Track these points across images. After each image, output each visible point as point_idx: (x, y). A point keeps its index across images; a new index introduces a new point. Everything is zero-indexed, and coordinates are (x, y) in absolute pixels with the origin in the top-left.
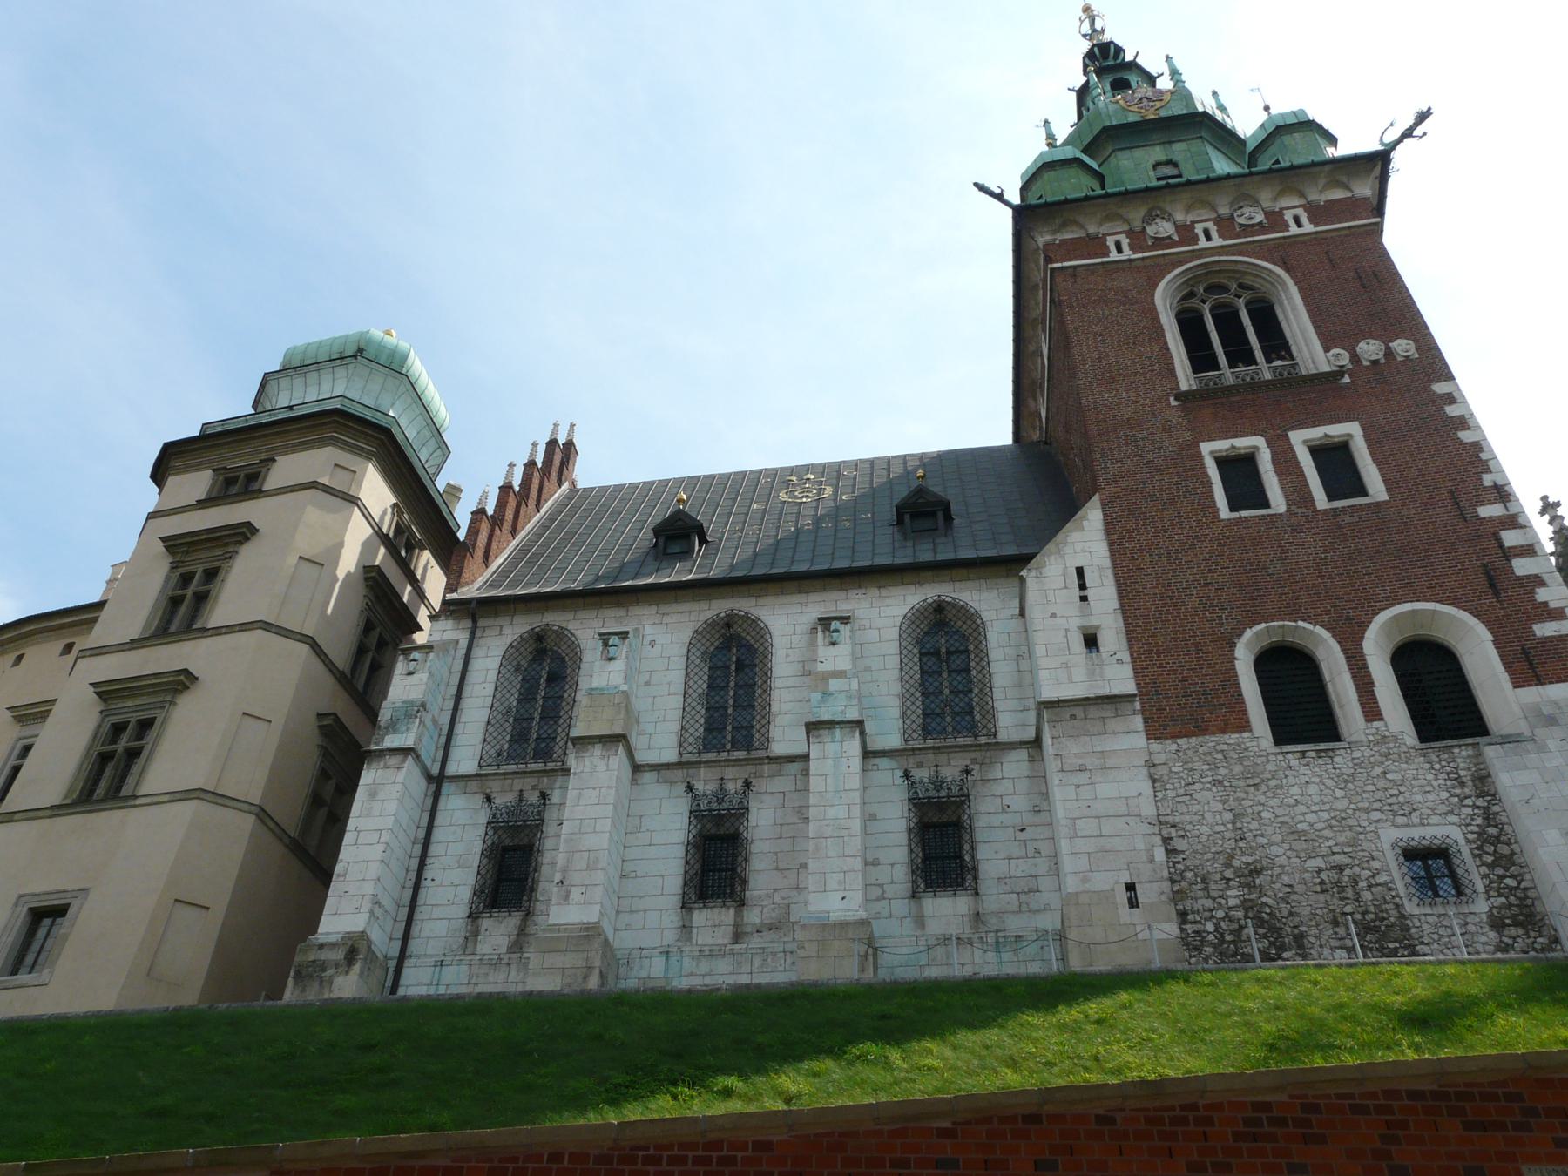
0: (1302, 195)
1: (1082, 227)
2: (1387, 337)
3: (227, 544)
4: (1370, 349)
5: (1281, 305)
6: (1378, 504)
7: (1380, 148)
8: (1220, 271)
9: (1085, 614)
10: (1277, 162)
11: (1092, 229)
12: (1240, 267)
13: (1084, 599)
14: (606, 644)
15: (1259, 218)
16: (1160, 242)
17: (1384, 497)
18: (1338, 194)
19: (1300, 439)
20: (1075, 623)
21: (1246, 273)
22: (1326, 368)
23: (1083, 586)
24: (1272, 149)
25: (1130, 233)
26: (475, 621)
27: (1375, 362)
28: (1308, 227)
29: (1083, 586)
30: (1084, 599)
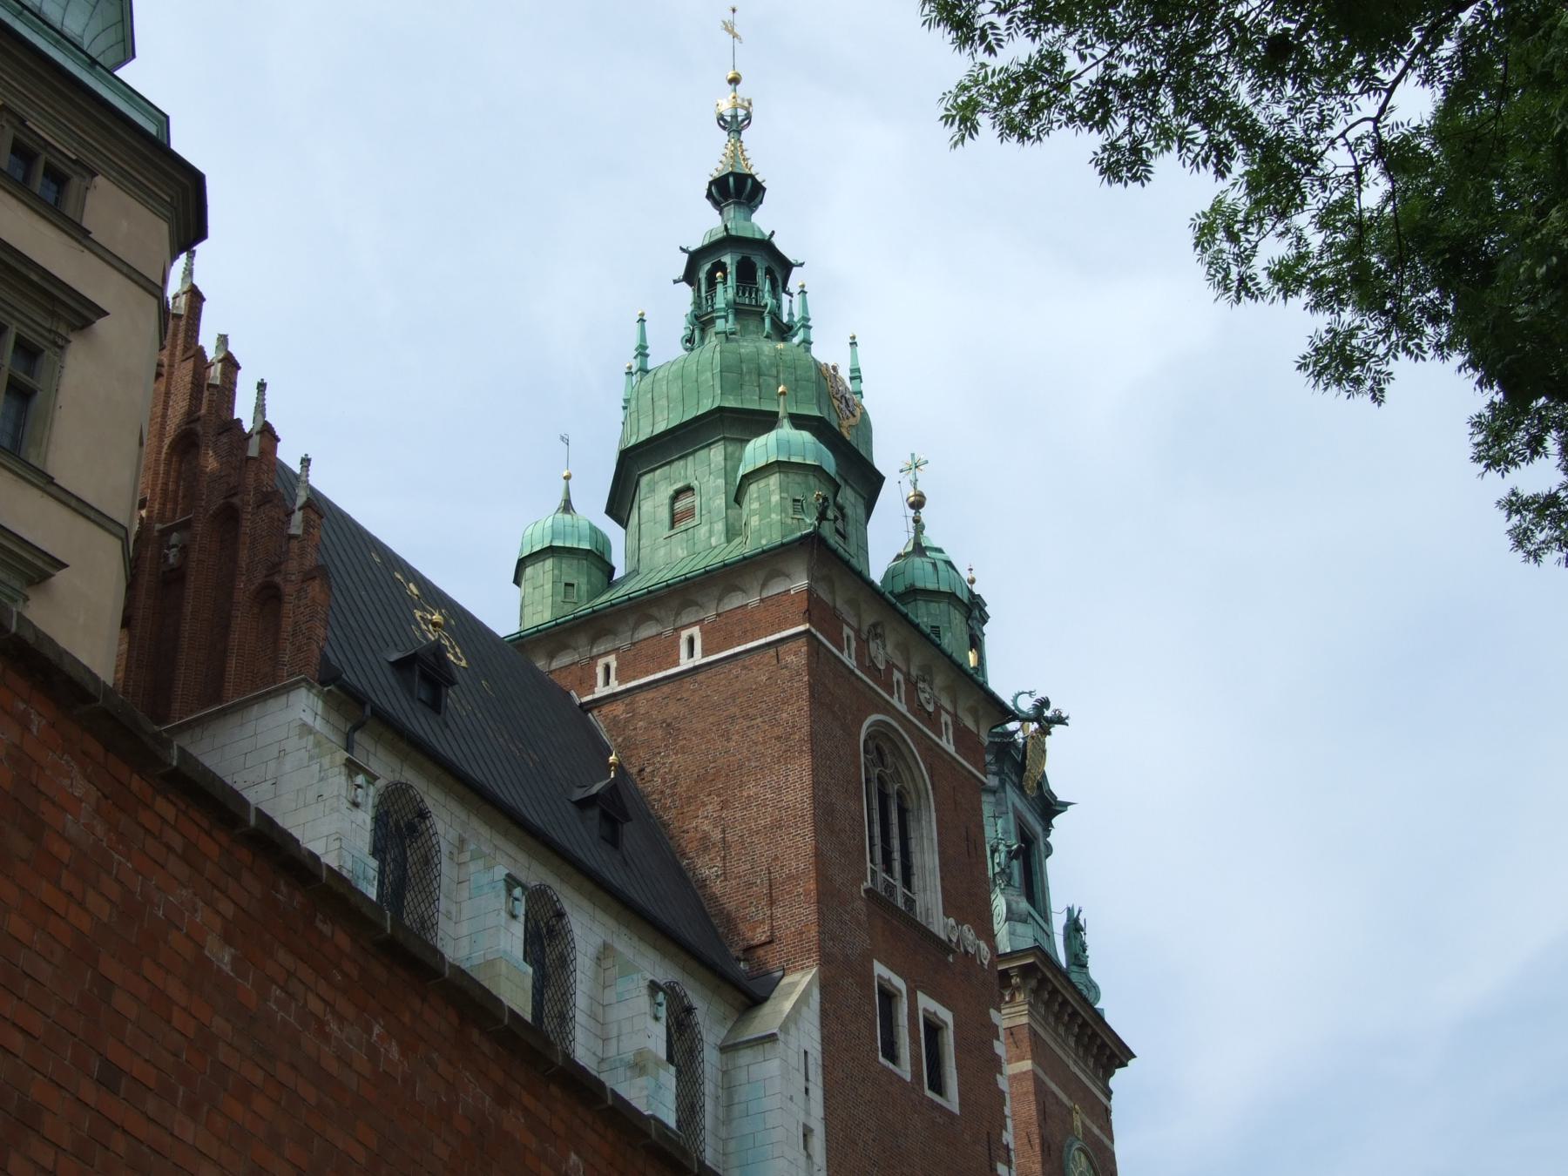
0: (954, 702)
1: (833, 592)
2: (978, 937)
3: (53, 314)
4: (969, 933)
5: (919, 821)
6: (950, 1114)
7: (1010, 703)
8: (890, 739)
9: (808, 1113)
10: (936, 629)
11: (838, 605)
12: (903, 748)
13: (807, 1090)
14: (509, 892)
15: (931, 708)
16: (872, 669)
17: (955, 1107)
18: (969, 723)
19: (925, 1002)
20: (802, 1118)
21: (904, 759)
22: (943, 936)
23: (807, 1079)
24: (934, 607)
25: (858, 632)
26: (355, 729)
27: (967, 952)
28: (951, 749)
29: (807, 1079)
30: (807, 1090)
